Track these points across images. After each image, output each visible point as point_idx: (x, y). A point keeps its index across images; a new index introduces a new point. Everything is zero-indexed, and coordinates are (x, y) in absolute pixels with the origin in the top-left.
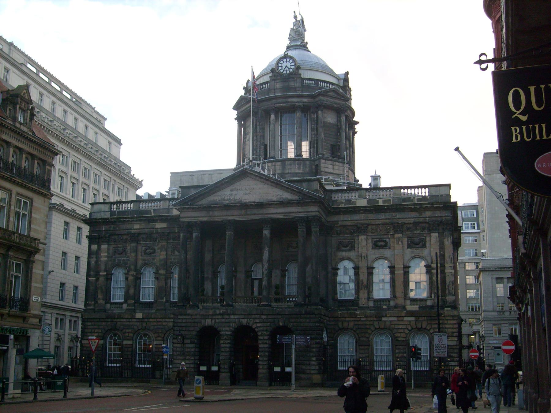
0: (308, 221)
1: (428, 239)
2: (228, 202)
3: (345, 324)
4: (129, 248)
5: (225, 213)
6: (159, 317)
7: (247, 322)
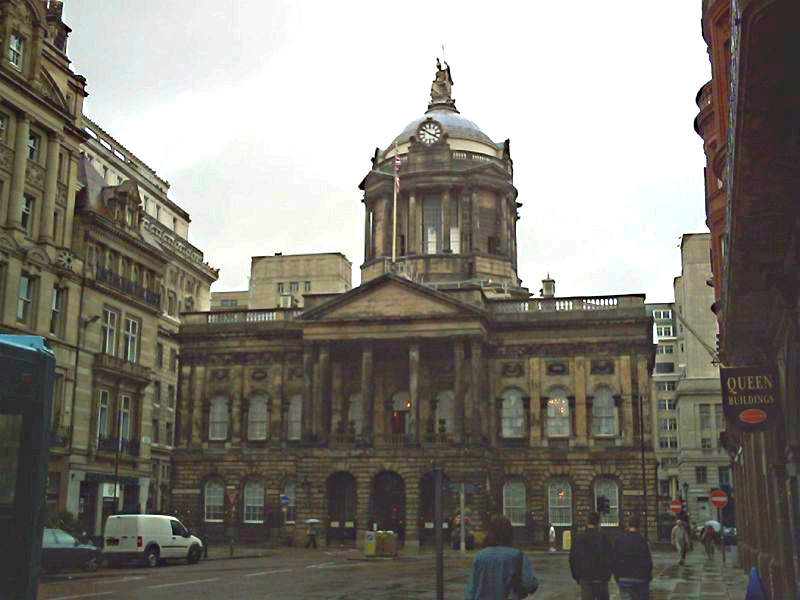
0: (467, 342)
1: (616, 363)
2: (364, 315)
3: (513, 470)
4: (232, 371)
5: (361, 329)
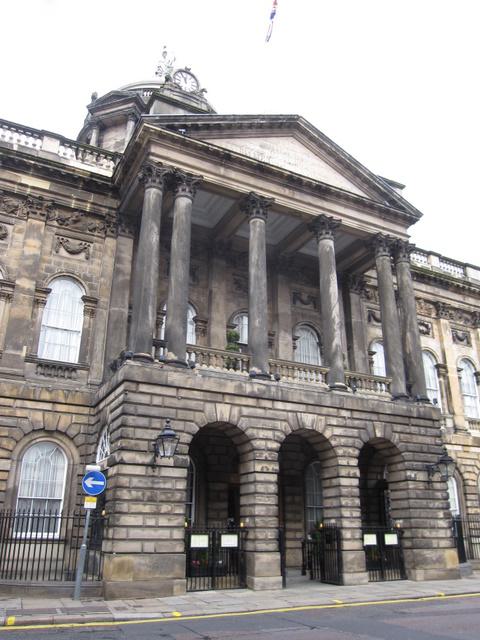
6: (7, 394)
7: (313, 421)
